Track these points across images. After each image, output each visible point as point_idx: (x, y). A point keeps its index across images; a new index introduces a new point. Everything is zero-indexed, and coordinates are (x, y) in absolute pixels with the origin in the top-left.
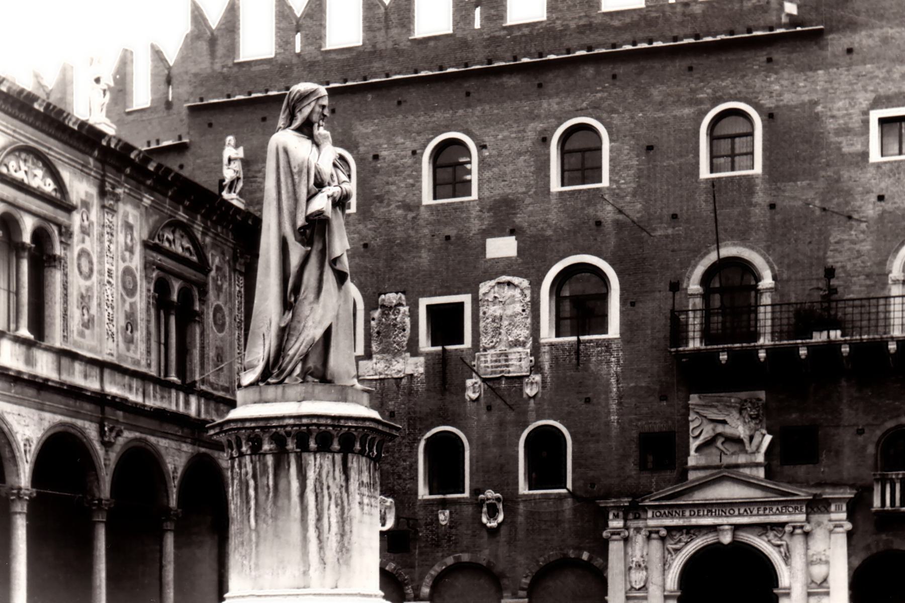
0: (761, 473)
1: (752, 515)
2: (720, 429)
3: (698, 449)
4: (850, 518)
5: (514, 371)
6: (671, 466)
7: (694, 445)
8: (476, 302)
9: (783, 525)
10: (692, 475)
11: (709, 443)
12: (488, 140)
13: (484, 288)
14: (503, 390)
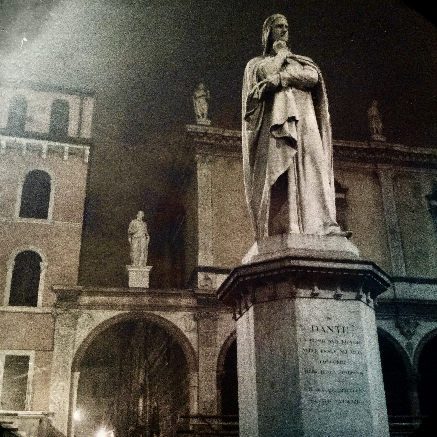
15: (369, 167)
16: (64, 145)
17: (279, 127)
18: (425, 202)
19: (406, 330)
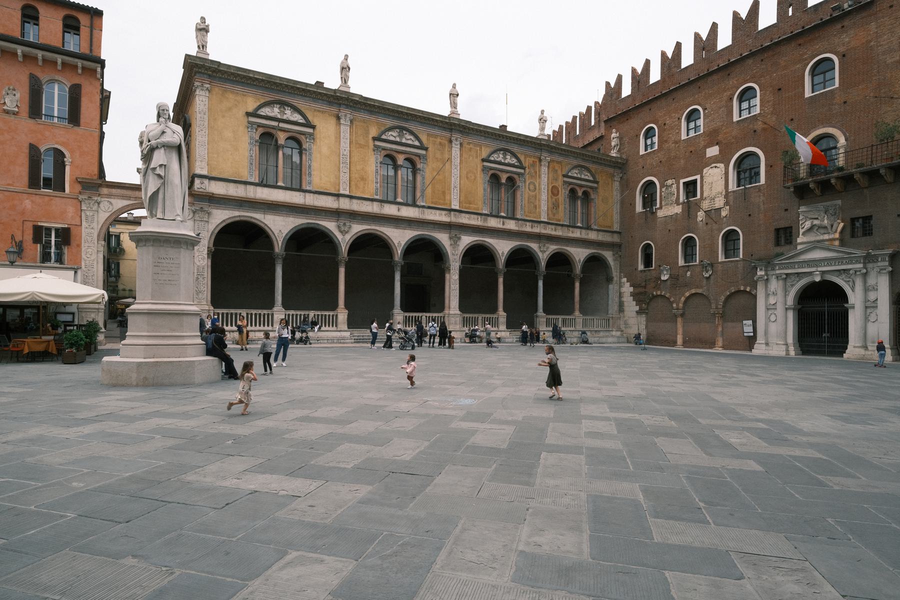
0: (837, 243)
1: (831, 265)
2: (816, 222)
3: (804, 234)
4: (891, 265)
5: (717, 206)
6: (791, 243)
7: (801, 231)
8: (702, 177)
9: (850, 270)
10: (799, 247)
11: (810, 229)
12: (708, 106)
13: (705, 171)
14: (713, 214)
15: (334, 110)
16: (76, 60)
17: (154, 169)
18: (371, 141)
19: (343, 228)
